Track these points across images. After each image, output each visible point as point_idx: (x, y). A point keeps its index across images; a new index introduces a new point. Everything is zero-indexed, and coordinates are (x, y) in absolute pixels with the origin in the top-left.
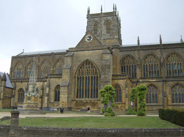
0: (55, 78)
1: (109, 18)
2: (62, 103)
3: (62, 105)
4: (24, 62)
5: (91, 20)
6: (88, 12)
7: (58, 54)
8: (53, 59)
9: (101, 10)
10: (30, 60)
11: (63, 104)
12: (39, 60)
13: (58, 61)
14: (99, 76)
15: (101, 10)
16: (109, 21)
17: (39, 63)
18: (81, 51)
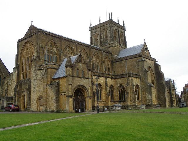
0: (135, 77)
1: (122, 31)
2: (154, 101)
3: (154, 102)
4: (58, 45)
5: (113, 26)
6: (109, 17)
7: (95, 49)
8: (90, 52)
9: (118, 21)
10: (67, 44)
11: (154, 102)
12: (77, 49)
13: (94, 56)
14: (154, 81)
15: (118, 21)
16: (121, 33)
17: (76, 51)
18: (146, 58)
